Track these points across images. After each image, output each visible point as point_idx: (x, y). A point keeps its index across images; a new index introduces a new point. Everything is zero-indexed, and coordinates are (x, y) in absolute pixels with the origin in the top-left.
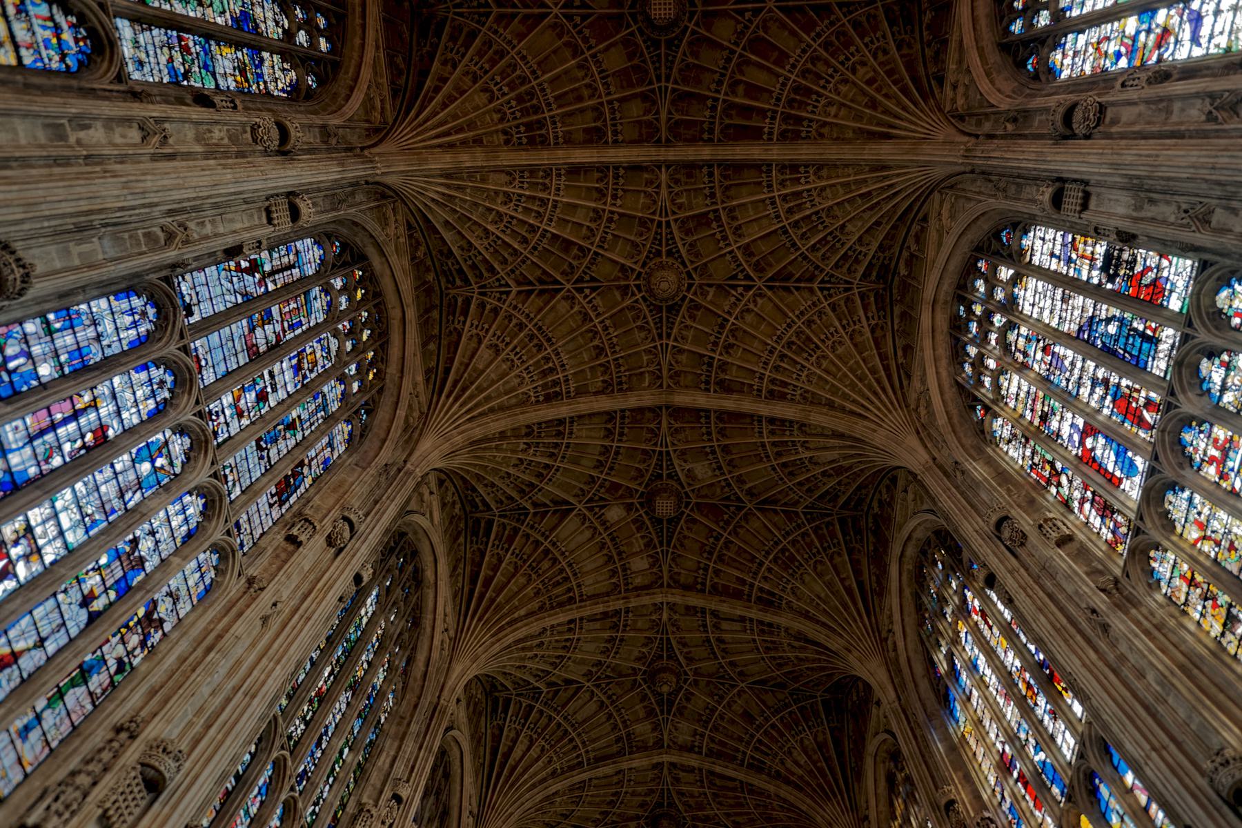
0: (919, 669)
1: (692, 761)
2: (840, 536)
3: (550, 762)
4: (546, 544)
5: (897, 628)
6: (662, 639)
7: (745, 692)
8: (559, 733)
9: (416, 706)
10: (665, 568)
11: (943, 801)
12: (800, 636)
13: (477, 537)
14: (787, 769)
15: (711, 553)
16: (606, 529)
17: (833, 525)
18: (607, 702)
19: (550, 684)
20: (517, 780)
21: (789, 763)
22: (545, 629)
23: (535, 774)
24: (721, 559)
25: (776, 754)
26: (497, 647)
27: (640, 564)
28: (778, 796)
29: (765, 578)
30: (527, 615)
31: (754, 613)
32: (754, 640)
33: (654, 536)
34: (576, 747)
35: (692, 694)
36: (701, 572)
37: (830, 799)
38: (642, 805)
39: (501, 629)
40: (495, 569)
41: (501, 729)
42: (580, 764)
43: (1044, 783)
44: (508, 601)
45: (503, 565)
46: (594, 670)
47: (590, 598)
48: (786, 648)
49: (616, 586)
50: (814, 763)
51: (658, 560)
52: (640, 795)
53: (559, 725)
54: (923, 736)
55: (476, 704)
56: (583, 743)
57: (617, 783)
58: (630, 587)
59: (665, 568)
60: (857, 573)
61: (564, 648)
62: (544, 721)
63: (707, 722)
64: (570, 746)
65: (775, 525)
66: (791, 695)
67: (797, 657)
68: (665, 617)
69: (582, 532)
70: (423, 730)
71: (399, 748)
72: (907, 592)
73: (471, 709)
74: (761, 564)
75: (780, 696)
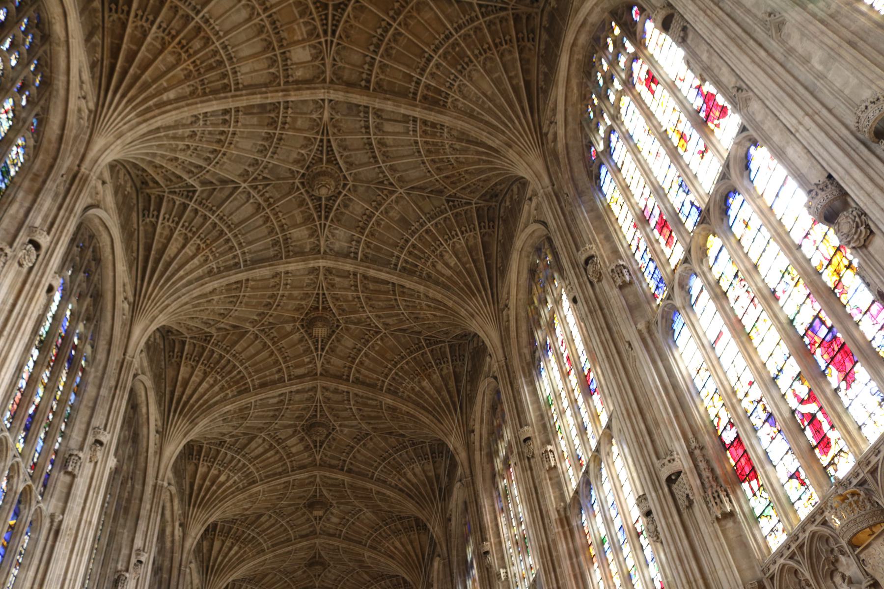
0: (575, 155)
1: (348, 266)
2: (513, 33)
3: (206, 260)
4: (197, 19)
5: (560, 118)
6: (322, 141)
7: (402, 198)
8: (215, 233)
9: (51, 167)
10: (328, 61)
11: (584, 258)
12: (463, 137)
13: (117, 5)
14: (438, 272)
15: (378, 46)
16: (265, 10)
17: (507, 20)
18: (264, 204)
20: (173, 275)
21: (440, 266)
23: (191, 272)
24: (388, 53)
26: (144, 128)
27: (301, 54)
28: (427, 296)
29: (433, 75)
30: (177, 100)
31: (418, 113)
32: (416, 142)
33: (318, 24)
35: (350, 200)
36: (366, 67)
37: (474, 295)
38: (297, 309)
39: (148, 110)
40: (140, 43)
41: (154, 226)
42: (237, 265)
43: (680, 220)
44: (155, 81)
45: (149, 39)
46: (251, 169)
47: (246, 87)
49: (275, 77)
50: (463, 265)
51: (321, 52)
52: (296, 299)
53: (215, 225)
54: (571, 212)
55: (125, 196)
56: (240, 244)
57: (275, 286)
58: (291, 79)
59: (328, 61)
60: (526, 71)
61: (219, 141)
62: (198, 220)
63: (364, 229)
64: (226, 247)
65: (447, 17)
66: (448, 201)
68: (326, 116)
69: (238, 10)
70: (62, 190)
71: (34, 202)
72: (574, 82)
73: (120, 195)
74: (429, 60)
75: (437, 203)
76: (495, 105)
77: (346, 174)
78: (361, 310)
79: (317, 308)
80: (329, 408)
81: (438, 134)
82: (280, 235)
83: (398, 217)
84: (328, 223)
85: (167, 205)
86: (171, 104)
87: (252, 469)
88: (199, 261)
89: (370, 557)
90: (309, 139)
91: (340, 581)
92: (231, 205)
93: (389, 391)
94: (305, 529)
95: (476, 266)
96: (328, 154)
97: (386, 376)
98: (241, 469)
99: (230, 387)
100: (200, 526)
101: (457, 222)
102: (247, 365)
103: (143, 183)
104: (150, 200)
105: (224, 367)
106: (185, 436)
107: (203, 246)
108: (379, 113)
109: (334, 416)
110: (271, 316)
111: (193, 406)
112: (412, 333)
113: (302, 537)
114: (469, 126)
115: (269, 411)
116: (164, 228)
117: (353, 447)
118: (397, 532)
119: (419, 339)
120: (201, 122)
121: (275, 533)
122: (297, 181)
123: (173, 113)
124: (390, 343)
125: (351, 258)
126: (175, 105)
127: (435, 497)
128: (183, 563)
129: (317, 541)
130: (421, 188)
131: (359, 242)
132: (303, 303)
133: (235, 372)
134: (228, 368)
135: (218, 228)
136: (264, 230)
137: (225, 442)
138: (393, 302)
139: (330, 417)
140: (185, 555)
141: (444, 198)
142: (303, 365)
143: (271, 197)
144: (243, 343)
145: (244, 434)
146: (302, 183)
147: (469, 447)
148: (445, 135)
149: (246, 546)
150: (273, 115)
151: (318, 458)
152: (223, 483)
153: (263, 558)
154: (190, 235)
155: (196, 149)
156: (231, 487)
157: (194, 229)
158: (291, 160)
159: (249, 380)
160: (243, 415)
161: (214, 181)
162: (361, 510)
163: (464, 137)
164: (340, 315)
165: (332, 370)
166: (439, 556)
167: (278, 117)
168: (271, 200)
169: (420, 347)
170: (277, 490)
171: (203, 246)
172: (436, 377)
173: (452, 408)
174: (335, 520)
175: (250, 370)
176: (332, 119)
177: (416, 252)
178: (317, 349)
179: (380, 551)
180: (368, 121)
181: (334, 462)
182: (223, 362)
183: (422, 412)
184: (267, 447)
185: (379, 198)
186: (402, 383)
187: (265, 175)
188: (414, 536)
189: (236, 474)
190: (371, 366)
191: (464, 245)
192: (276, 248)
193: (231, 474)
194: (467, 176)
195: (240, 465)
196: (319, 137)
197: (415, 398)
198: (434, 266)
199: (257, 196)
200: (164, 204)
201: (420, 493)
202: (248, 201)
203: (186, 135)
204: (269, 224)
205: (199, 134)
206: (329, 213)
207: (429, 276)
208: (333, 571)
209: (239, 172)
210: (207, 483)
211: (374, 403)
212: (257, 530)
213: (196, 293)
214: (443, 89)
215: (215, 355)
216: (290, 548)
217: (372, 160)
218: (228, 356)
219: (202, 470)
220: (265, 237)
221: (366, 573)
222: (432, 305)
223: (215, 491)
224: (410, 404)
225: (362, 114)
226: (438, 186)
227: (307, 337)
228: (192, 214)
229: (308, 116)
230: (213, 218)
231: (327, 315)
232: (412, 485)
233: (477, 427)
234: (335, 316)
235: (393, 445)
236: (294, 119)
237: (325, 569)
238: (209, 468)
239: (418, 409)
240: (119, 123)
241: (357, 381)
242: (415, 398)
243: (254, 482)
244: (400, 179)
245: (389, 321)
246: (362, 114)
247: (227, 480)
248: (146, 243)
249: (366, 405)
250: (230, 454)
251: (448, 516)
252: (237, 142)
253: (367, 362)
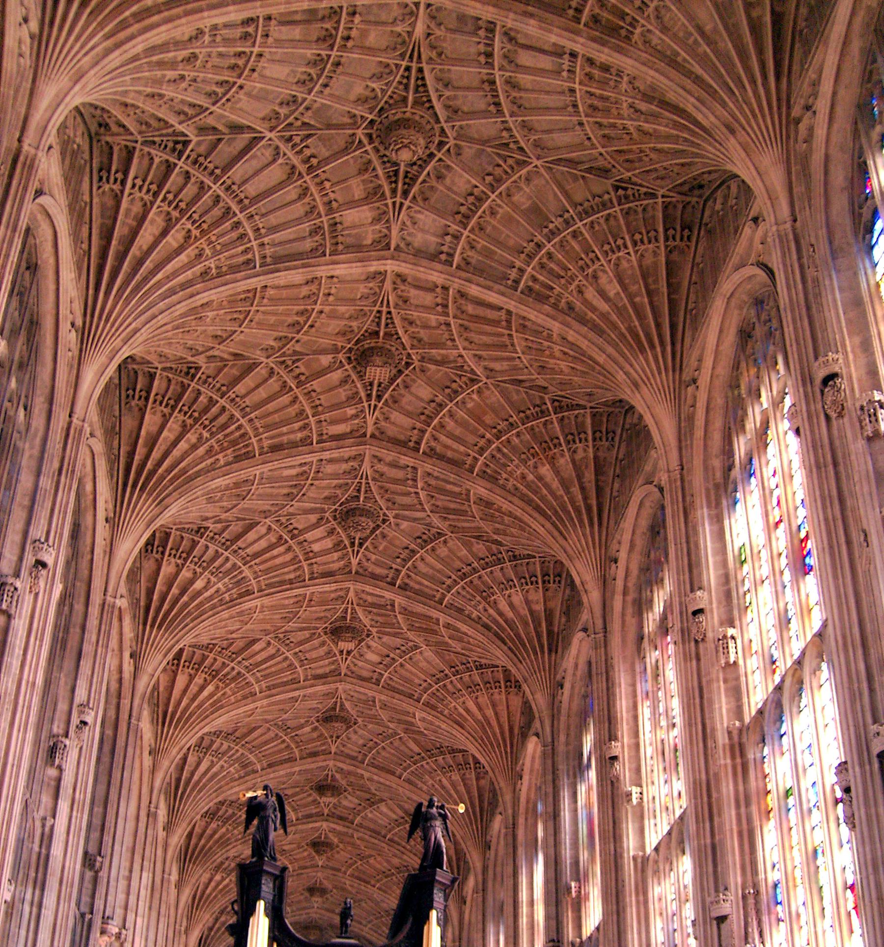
6: (408, 69)
8: (217, 212)
14: (586, 302)
18: (302, 168)
19: (202, 130)
20: (146, 280)
21: (590, 293)
22: (200, 32)
23: (175, 274)
25: (572, 278)
31: (580, 45)
32: (572, 91)
34: (242, 236)
35: (448, 167)
37: (642, 350)
46: (283, 111)
48: (625, 112)
50: (631, 297)
52: (341, 317)
53: (217, 199)
55: (75, 154)
62: (191, 190)
63: (467, 217)
64: (234, 235)
66: (616, 188)
67: (639, 129)
75: (597, 190)
76: (715, 52)
77: (445, 126)
78: (449, 343)
79: (377, 333)
80: (381, 487)
81: (612, 83)
82: (324, 219)
83: (527, 205)
84: (407, 203)
85: (140, 163)
86: (160, 12)
87: (247, 573)
88: (188, 256)
89: (423, 720)
90: (387, 66)
91: (371, 749)
92: (247, 165)
93: (483, 474)
94: (325, 666)
95: (651, 303)
96: (416, 91)
97: (482, 451)
98: (228, 573)
99: (223, 450)
100: (160, 657)
101: (628, 225)
102: (252, 415)
103: (100, 125)
104: (111, 154)
105: (215, 418)
106: (148, 526)
107: (195, 232)
108: (513, 34)
109: (388, 500)
110: (298, 341)
111: (163, 478)
112: (531, 388)
113: (317, 677)
114: (666, 81)
115: (282, 487)
116: (132, 201)
117: (414, 552)
118: (471, 687)
119: (542, 398)
120: (207, 38)
121: (273, 669)
122: (360, 133)
123: (163, 28)
124: (493, 399)
125: (440, 262)
126: (166, 14)
127: (542, 647)
129: (341, 687)
130: (572, 163)
131: (457, 237)
132: (355, 324)
133: (233, 427)
134: (222, 419)
135: (221, 204)
136: (299, 209)
137: (206, 528)
138: (505, 339)
139: (382, 503)
141: (611, 181)
142: (345, 420)
143: (314, 157)
144: (249, 381)
145: (239, 519)
146: (370, 136)
147: (605, 582)
148: (624, 86)
149: (227, 685)
150: (328, 26)
151: (354, 562)
152: (199, 593)
153: (252, 706)
154: (175, 214)
155: (195, 81)
156: (211, 598)
157: (183, 205)
158: (352, 97)
159: (254, 440)
160: (240, 490)
161: (221, 127)
162: (417, 647)
163: (656, 95)
164: (413, 347)
165: (392, 431)
166: (537, 735)
167: (336, 29)
168: (314, 161)
169: (542, 412)
170: (284, 607)
171: (195, 232)
172: (564, 462)
173: (585, 517)
175: (258, 424)
176: (429, 35)
177: (552, 265)
178: (369, 396)
179: (441, 713)
180: (491, 45)
181: (378, 571)
182: (215, 410)
183: (536, 515)
184: (274, 540)
185: (498, 171)
186: (505, 466)
187: (307, 120)
188: (500, 697)
189: (220, 580)
190: (458, 431)
191: (635, 264)
192: (316, 238)
193: (213, 579)
194: (653, 156)
195: (228, 565)
196: (404, 64)
197: (525, 491)
198: (580, 292)
199: (290, 154)
200: (135, 161)
201: (518, 636)
202: (274, 160)
203: (180, 59)
204: (307, 200)
205: (201, 57)
206: (410, 186)
207: (571, 307)
208: (361, 732)
209: (261, 115)
210: (175, 591)
211: (457, 489)
212: (246, 663)
213: (181, 308)
214: (627, 10)
215: (201, 398)
216: (296, 694)
217: (492, 108)
218: (222, 402)
219: (167, 569)
220: (298, 221)
221: (416, 741)
222: (571, 353)
223: (186, 605)
224: (516, 500)
225: (482, 33)
226: (601, 163)
227: (354, 377)
228: (181, 180)
229: (389, 29)
230: (214, 187)
231: (392, 346)
232: (506, 621)
233: (623, 556)
234: (404, 348)
235: (481, 555)
236: (364, 34)
237: (348, 728)
238: (179, 569)
239: (529, 509)
240: (77, 53)
241: (432, 453)
242: (525, 491)
243: (249, 593)
244: (537, 145)
245: (497, 366)
246: (482, 33)
247: (206, 588)
248: (102, 225)
249: (443, 491)
250: (212, 548)
251: (558, 677)
252: (264, 67)
253: (451, 425)
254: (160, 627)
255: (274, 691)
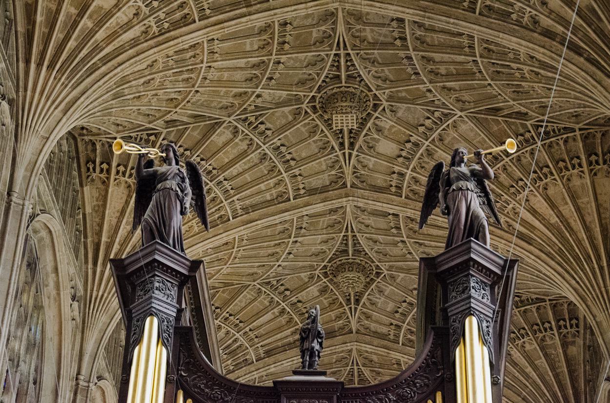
113: (312, 192)
121: (248, 177)
128: (17, 188)
129: (349, 204)
140: (20, 173)
156: (128, 26)
174: (387, 147)
208: (389, 289)
216: (286, 216)
223: (92, 33)
237: (367, 285)
243: (186, 21)
254: (51, 66)
255: (253, 215)
